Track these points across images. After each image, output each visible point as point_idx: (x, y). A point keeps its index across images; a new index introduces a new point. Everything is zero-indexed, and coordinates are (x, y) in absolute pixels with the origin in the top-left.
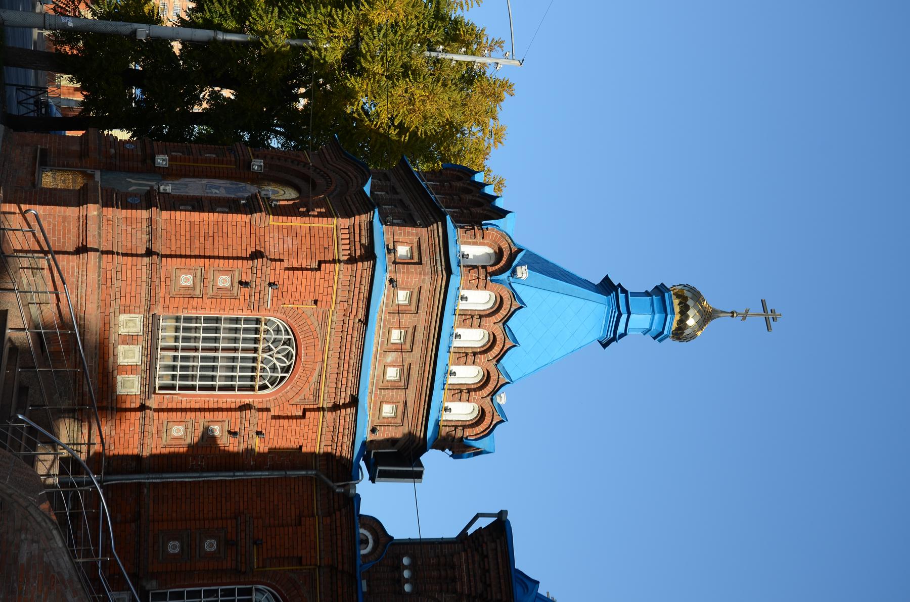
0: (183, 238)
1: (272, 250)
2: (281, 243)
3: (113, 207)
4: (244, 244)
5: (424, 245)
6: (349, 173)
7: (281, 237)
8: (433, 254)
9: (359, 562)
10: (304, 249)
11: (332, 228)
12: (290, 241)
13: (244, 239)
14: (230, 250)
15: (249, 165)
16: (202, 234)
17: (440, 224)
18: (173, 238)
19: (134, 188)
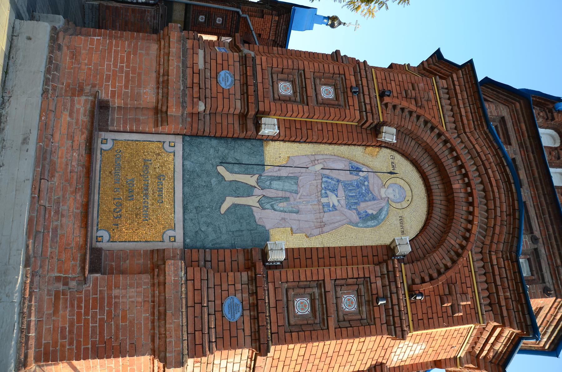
3: (204, 355)
6: (490, 171)
19: (229, 202)
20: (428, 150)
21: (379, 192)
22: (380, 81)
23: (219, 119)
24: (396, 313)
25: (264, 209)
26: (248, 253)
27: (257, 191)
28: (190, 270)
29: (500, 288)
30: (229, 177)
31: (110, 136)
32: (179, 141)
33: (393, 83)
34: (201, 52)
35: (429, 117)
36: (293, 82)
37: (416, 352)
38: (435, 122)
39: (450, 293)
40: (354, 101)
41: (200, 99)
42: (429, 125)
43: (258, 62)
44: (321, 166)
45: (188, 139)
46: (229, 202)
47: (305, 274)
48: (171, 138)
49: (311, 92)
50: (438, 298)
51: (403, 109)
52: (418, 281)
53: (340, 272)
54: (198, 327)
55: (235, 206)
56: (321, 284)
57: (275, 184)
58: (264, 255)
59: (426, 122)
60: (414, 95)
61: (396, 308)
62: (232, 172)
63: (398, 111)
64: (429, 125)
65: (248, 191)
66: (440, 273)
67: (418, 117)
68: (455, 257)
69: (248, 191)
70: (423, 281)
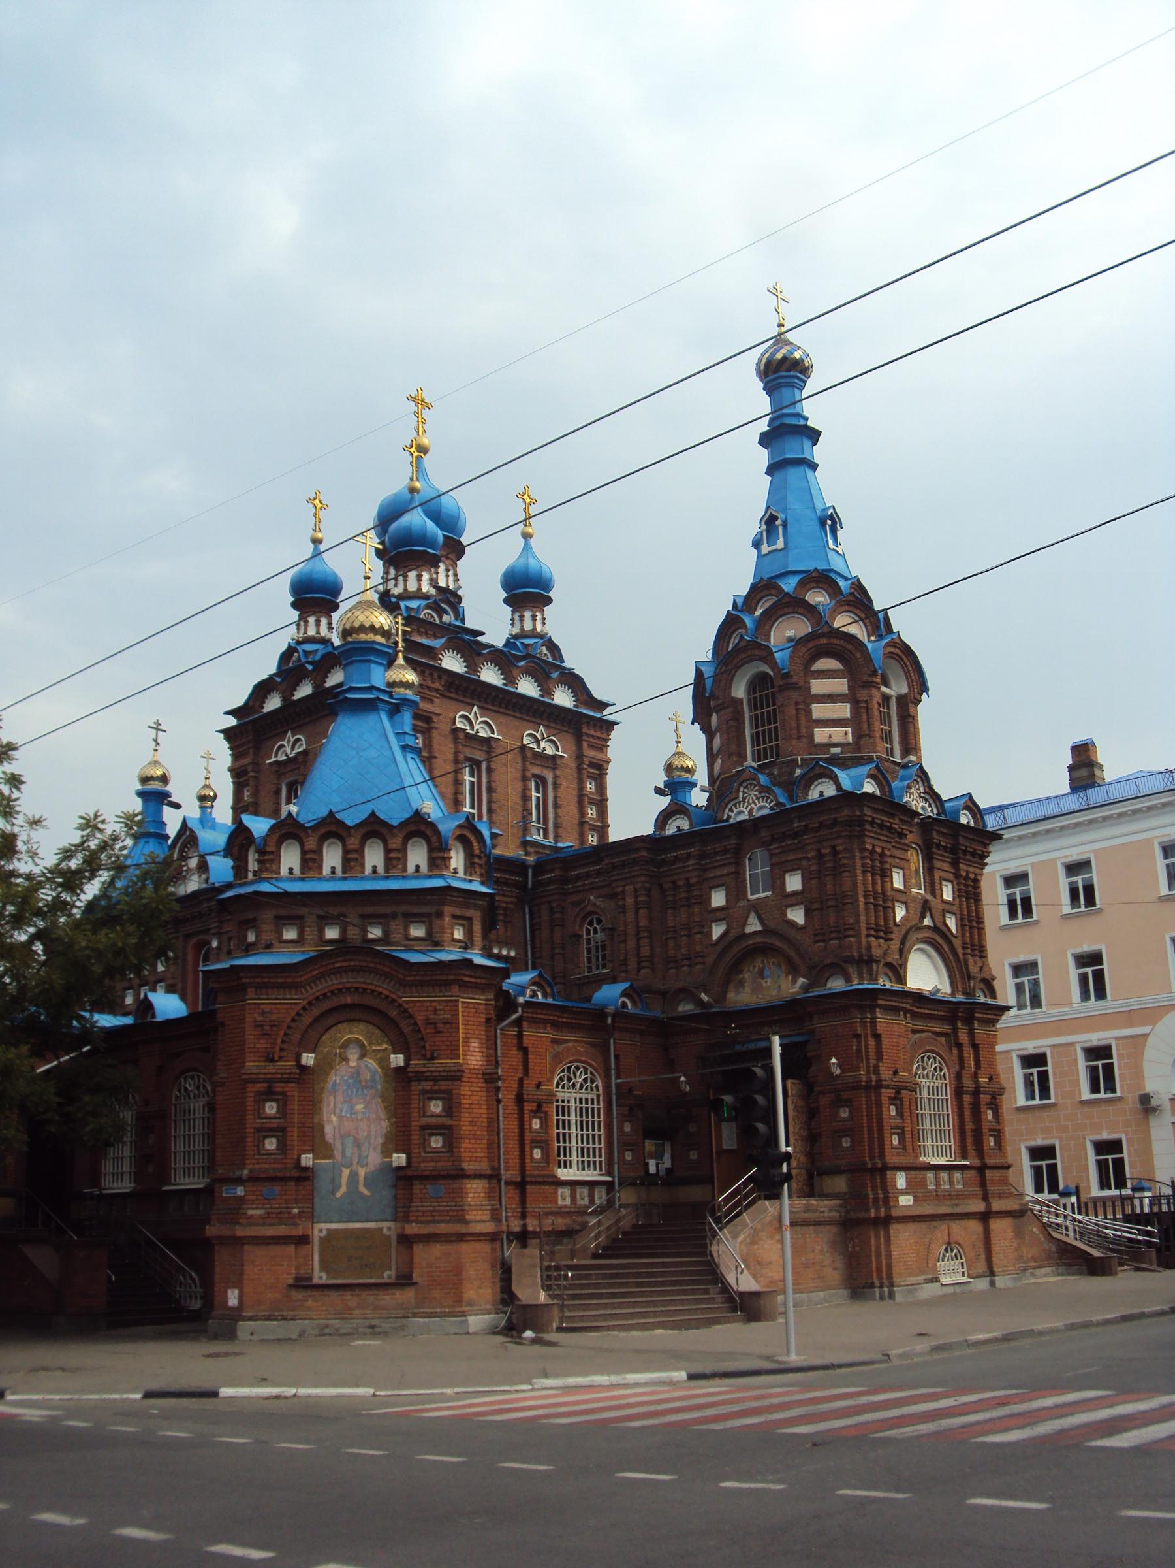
0: (475, 1146)
1: (480, 1063)
2: (475, 1054)
4: (478, 1089)
5: (458, 912)
7: (470, 1053)
8: (467, 906)
9: (550, 1001)
10: (477, 1032)
11: (463, 1002)
12: (473, 1044)
13: (472, 1089)
14: (482, 1102)
15: (304, 1068)
16: (471, 1128)
17: (450, 893)
18: (475, 1155)
19: (362, 1189)
20: (317, 1019)
21: (352, 1067)
22: (256, 1059)
23: (301, 1197)
24: (445, 1074)
25: (367, 1164)
26: (398, 1178)
27: (355, 1167)
28: (411, 1218)
29: (433, 978)
30: (343, 1189)
31: (316, 1274)
32: (317, 1226)
33: (257, 1046)
34: (250, 1212)
35: (289, 1019)
36: (265, 1137)
37: (476, 1045)
38: (293, 1013)
39: (435, 1024)
40: (279, 1087)
41: (289, 1213)
42: (296, 1018)
43: (251, 1166)
44: (333, 1116)
45: (315, 1220)
46: (362, 1189)
47: (415, 1139)
48: (316, 1232)
49: (275, 1123)
50: (440, 1035)
51: (283, 1042)
52: (423, 1052)
53: (415, 1114)
54: (446, 1213)
55: (365, 1185)
56: (423, 1128)
57: (348, 1154)
58: (399, 1168)
59: (293, 1020)
60: (268, 1028)
61: (442, 1074)
62: (340, 1186)
63: (285, 1046)
64: (296, 1018)
65: (354, 1176)
66: (419, 1031)
67: (289, 1027)
68: (407, 1014)
69: (354, 1176)
70: (424, 1047)
